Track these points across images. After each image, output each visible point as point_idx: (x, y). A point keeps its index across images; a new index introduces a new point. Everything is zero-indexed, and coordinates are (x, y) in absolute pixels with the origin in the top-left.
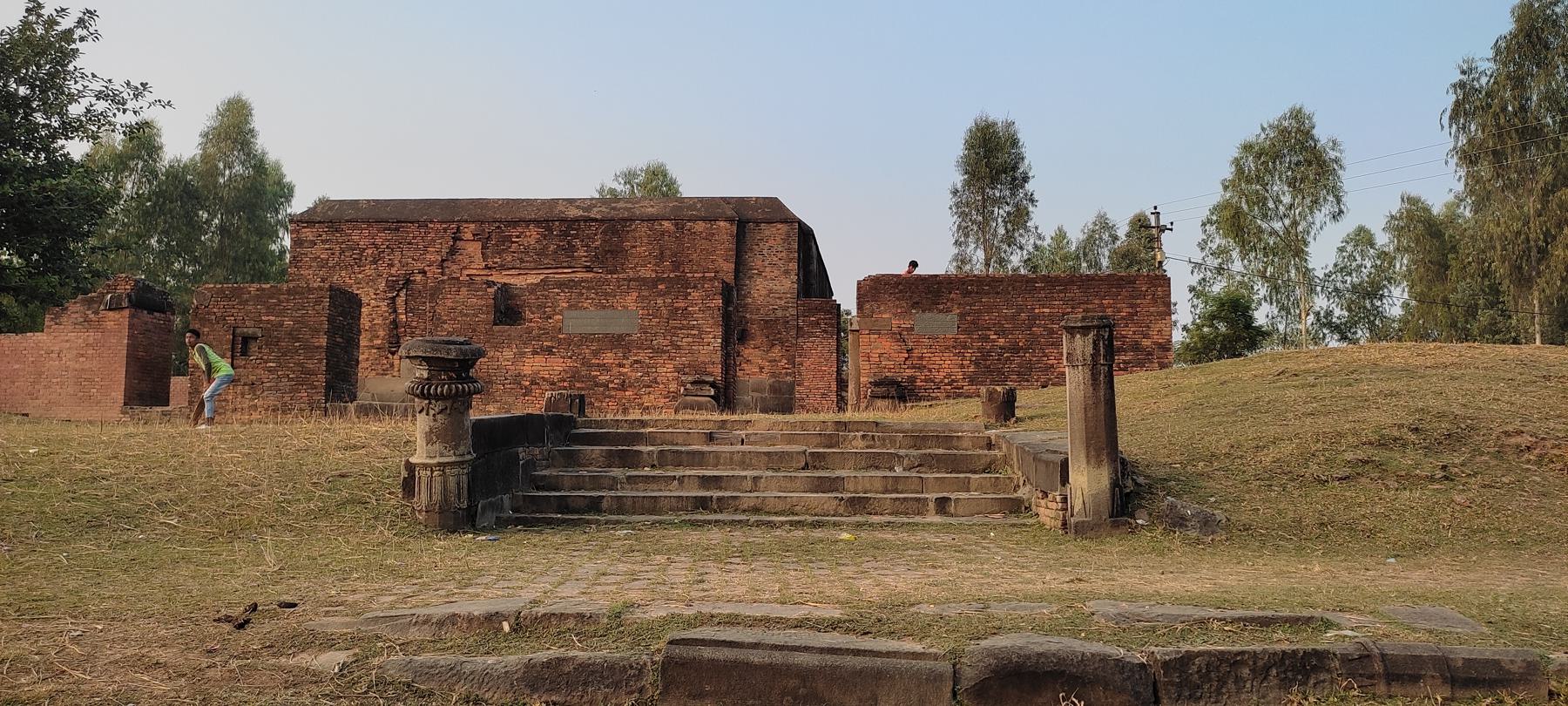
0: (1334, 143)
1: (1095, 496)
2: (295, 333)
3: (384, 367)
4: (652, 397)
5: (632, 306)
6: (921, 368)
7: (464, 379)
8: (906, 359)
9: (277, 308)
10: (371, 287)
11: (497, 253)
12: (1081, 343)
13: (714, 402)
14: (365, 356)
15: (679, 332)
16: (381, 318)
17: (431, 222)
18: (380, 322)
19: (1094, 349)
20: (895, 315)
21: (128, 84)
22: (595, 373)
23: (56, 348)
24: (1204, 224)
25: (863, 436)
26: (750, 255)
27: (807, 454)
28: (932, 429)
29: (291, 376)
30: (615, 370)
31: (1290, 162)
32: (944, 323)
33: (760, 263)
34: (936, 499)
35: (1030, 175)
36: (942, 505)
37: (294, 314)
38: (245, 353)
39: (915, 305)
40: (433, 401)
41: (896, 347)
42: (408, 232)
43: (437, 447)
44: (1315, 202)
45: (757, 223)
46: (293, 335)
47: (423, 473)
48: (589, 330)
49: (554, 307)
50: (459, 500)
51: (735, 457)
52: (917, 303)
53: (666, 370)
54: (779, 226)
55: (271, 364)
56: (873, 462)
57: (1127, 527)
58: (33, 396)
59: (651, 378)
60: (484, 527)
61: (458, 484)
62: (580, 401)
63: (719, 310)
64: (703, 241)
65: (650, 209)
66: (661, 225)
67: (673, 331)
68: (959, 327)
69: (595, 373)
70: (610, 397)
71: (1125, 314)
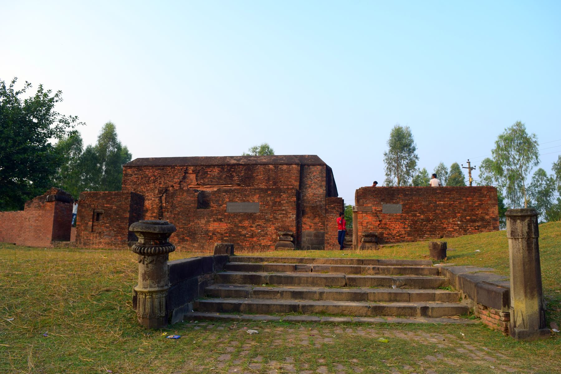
0: (534, 135)
1: (530, 316)
2: (117, 212)
4: (265, 241)
5: (256, 201)
6: (385, 229)
7: (164, 244)
8: (379, 224)
9: (110, 201)
10: (152, 192)
11: (202, 178)
12: (521, 225)
13: (293, 244)
15: (277, 212)
16: (156, 205)
17: (176, 166)
19: (528, 229)
20: (374, 205)
21: (70, 116)
22: (240, 230)
23: (28, 217)
24: (480, 168)
25: (374, 268)
26: (305, 179)
27: (346, 278)
28: (406, 263)
29: (115, 230)
30: (249, 229)
31: (517, 143)
32: (396, 208)
33: (310, 182)
34: (421, 308)
35: (416, 148)
36: (425, 311)
37: (117, 204)
38: (98, 220)
39: (383, 200)
40: (147, 257)
41: (374, 219)
42: (167, 170)
43: (148, 282)
44: (528, 158)
45: (309, 165)
46: (116, 212)
47: (141, 296)
48: (238, 211)
49: (223, 201)
50: (160, 311)
51: (309, 280)
52: (383, 199)
53: (271, 229)
54: (318, 167)
55: (107, 225)
56: (381, 283)
57: (550, 334)
58: (19, 236)
59: (265, 233)
60: (177, 323)
61: (160, 303)
62: (231, 248)
63: (295, 202)
64: (286, 173)
65: (264, 160)
66: (269, 167)
67: (274, 212)
68: (402, 210)
69: (240, 230)
70: (247, 241)
71: (477, 204)
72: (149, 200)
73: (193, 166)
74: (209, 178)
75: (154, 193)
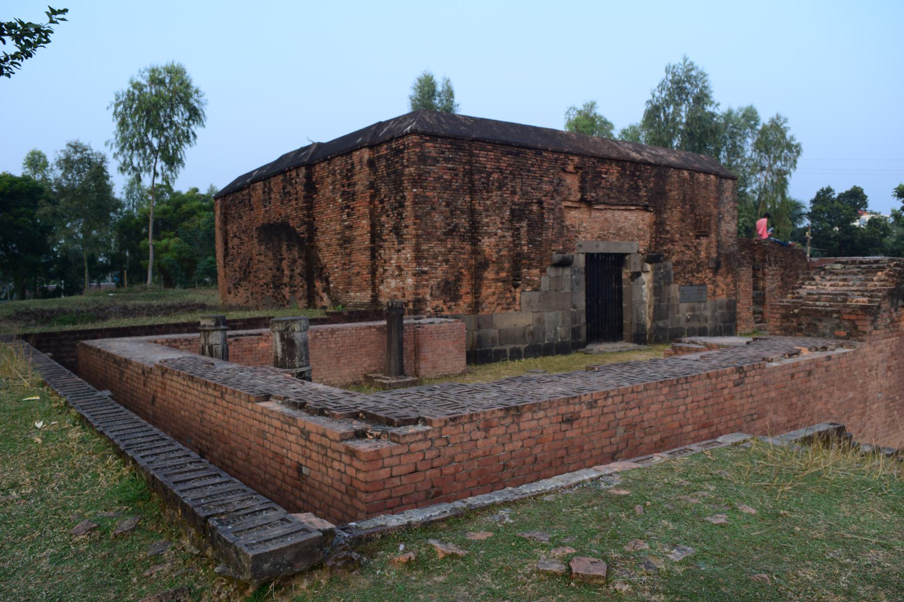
3: (508, 301)
10: (498, 215)
14: (490, 291)
16: (506, 249)
17: (546, 150)
18: (506, 253)
42: (527, 159)
72: (490, 235)
73: (577, 155)
74: (603, 188)
75: (502, 218)
